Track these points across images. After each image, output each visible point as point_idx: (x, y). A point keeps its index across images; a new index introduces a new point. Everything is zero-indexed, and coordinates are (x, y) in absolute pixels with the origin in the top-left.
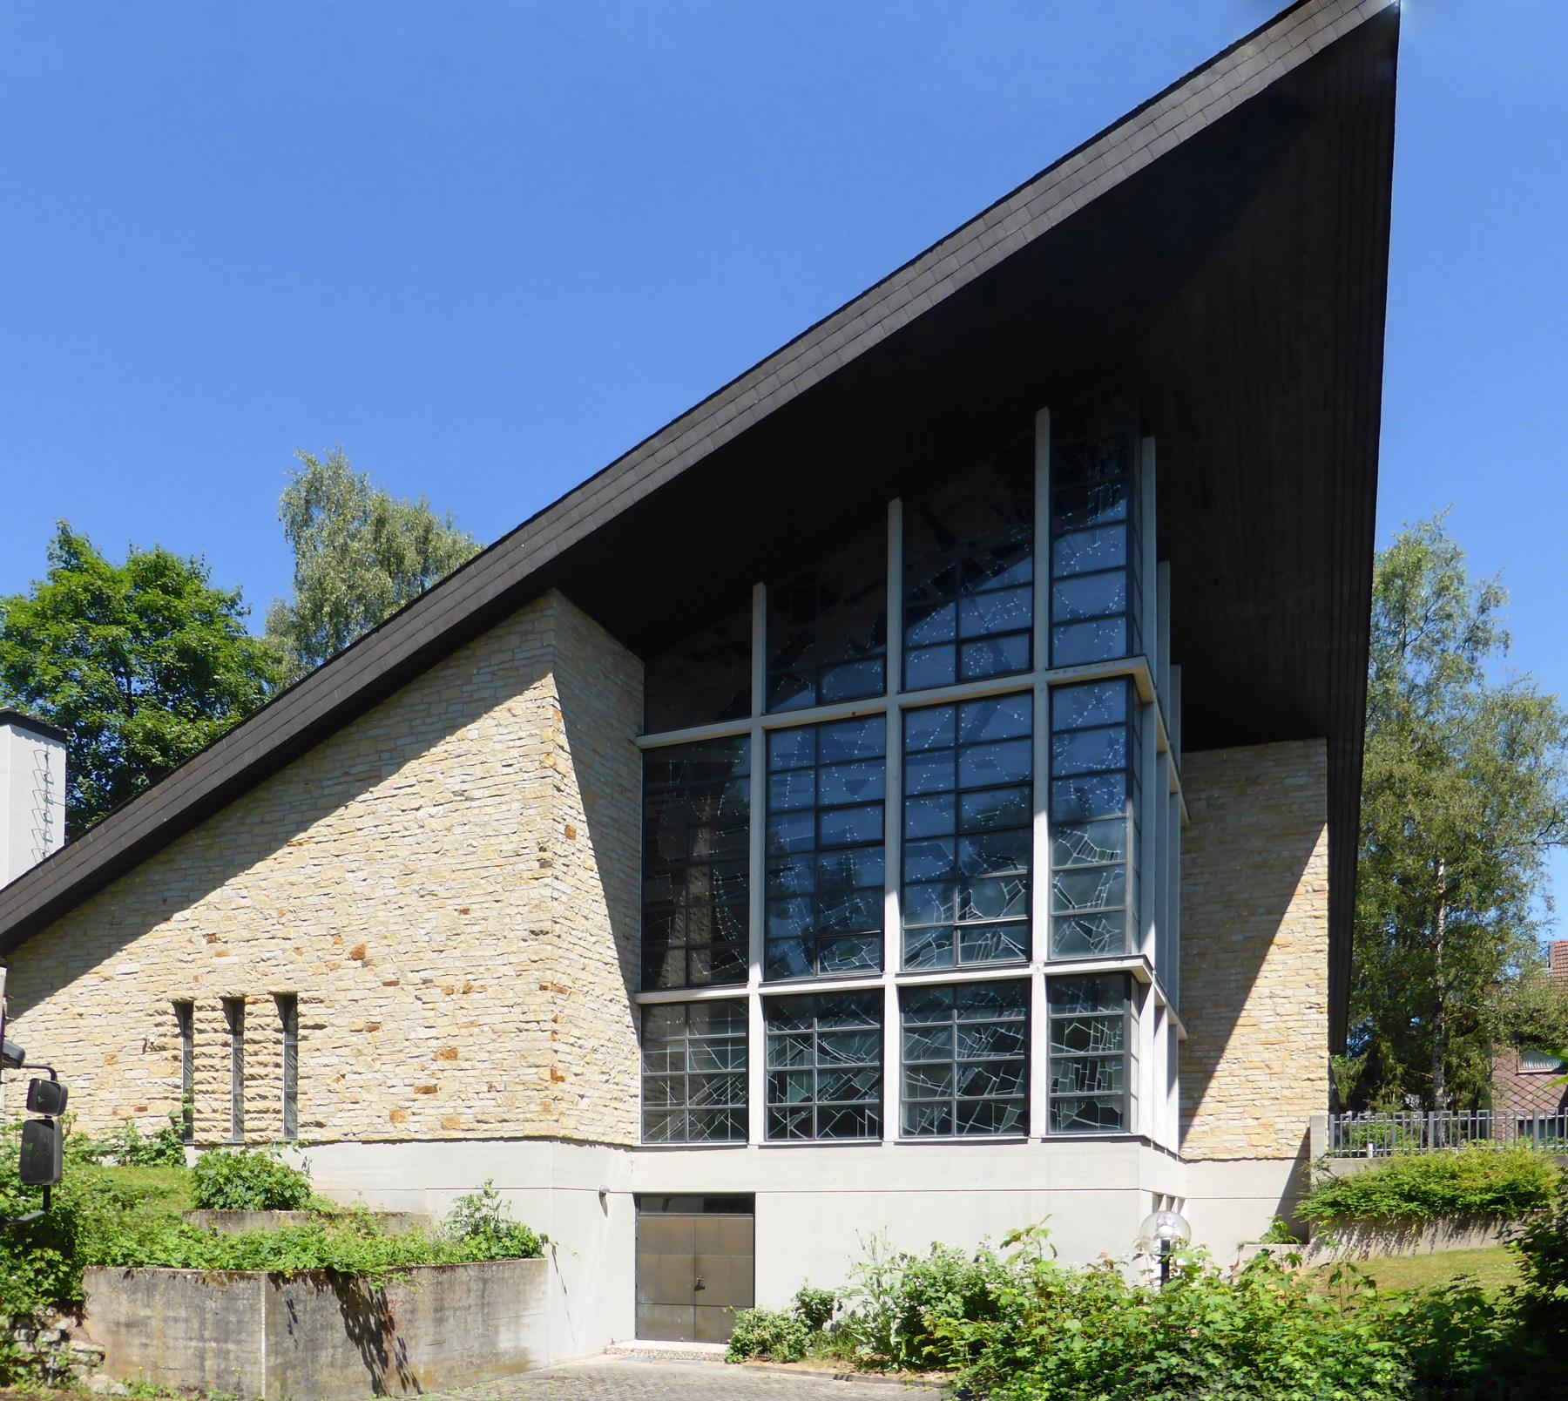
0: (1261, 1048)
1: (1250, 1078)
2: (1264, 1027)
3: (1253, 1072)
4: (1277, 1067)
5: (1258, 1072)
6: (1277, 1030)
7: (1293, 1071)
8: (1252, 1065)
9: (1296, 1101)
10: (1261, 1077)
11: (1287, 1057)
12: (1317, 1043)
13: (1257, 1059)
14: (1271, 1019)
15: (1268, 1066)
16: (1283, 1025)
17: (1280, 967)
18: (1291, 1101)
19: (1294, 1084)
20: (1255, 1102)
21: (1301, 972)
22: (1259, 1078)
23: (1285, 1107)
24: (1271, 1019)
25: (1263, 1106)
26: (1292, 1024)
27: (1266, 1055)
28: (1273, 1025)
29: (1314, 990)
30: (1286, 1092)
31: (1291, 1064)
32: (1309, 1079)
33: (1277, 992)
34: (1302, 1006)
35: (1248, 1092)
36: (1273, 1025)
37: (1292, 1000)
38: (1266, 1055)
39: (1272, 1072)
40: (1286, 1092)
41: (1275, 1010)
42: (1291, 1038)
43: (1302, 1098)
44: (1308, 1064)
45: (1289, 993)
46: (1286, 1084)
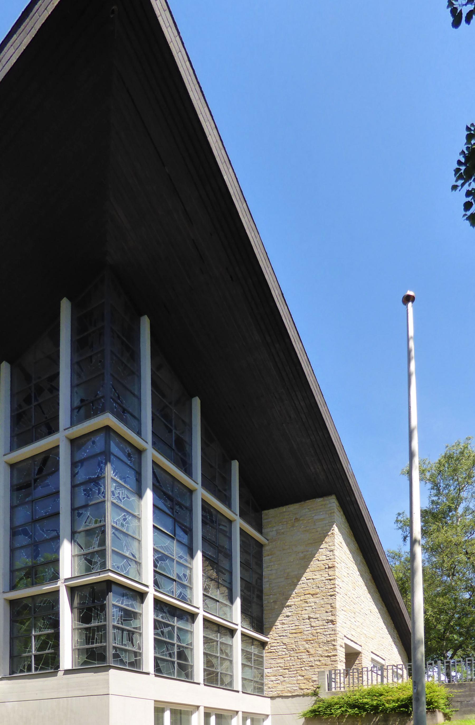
0: (304, 643)
1: (299, 657)
2: (305, 633)
3: (301, 654)
4: (312, 651)
5: (303, 654)
6: (312, 634)
7: (320, 652)
8: (300, 651)
9: (322, 667)
10: (305, 656)
11: (318, 646)
12: (332, 638)
13: (302, 648)
14: (309, 629)
15: (308, 651)
16: (315, 631)
17: (313, 604)
18: (319, 667)
19: (321, 659)
20: (302, 668)
21: (323, 606)
22: (303, 657)
23: (317, 670)
24: (309, 629)
25: (306, 669)
26: (319, 631)
27: (307, 646)
28: (310, 632)
29: (330, 613)
30: (318, 663)
31: (319, 649)
32: (328, 656)
33: (311, 616)
34: (324, 622)
35: (298, 664)
36: (310, 632)
37: (319, 619)
38: (307, 646)
39: (310, 653)
40: (318, 663)
41: (311, 625)
42: (319, 637)
43: (325, 665)
44: (328, 649)
45: (318, 616)
46: (316, 659)
